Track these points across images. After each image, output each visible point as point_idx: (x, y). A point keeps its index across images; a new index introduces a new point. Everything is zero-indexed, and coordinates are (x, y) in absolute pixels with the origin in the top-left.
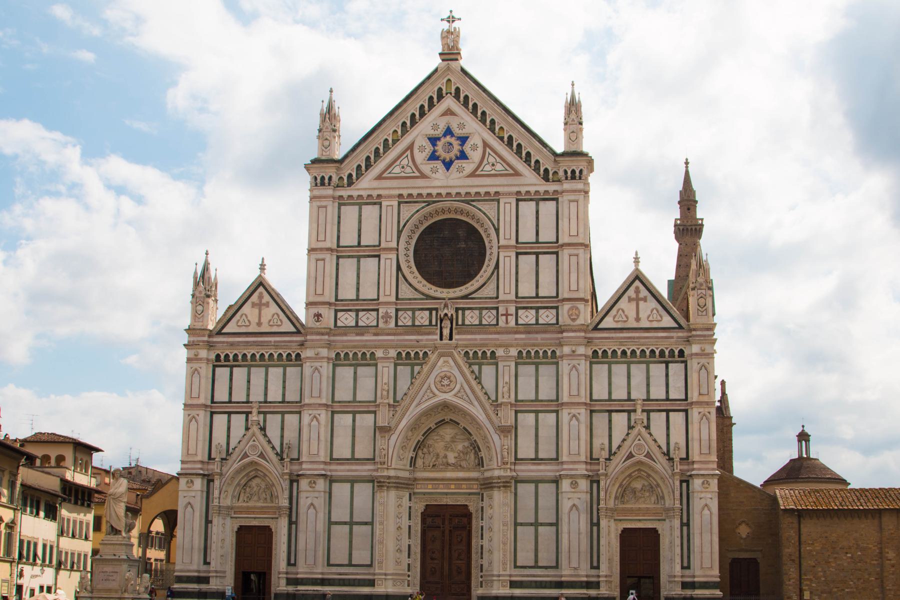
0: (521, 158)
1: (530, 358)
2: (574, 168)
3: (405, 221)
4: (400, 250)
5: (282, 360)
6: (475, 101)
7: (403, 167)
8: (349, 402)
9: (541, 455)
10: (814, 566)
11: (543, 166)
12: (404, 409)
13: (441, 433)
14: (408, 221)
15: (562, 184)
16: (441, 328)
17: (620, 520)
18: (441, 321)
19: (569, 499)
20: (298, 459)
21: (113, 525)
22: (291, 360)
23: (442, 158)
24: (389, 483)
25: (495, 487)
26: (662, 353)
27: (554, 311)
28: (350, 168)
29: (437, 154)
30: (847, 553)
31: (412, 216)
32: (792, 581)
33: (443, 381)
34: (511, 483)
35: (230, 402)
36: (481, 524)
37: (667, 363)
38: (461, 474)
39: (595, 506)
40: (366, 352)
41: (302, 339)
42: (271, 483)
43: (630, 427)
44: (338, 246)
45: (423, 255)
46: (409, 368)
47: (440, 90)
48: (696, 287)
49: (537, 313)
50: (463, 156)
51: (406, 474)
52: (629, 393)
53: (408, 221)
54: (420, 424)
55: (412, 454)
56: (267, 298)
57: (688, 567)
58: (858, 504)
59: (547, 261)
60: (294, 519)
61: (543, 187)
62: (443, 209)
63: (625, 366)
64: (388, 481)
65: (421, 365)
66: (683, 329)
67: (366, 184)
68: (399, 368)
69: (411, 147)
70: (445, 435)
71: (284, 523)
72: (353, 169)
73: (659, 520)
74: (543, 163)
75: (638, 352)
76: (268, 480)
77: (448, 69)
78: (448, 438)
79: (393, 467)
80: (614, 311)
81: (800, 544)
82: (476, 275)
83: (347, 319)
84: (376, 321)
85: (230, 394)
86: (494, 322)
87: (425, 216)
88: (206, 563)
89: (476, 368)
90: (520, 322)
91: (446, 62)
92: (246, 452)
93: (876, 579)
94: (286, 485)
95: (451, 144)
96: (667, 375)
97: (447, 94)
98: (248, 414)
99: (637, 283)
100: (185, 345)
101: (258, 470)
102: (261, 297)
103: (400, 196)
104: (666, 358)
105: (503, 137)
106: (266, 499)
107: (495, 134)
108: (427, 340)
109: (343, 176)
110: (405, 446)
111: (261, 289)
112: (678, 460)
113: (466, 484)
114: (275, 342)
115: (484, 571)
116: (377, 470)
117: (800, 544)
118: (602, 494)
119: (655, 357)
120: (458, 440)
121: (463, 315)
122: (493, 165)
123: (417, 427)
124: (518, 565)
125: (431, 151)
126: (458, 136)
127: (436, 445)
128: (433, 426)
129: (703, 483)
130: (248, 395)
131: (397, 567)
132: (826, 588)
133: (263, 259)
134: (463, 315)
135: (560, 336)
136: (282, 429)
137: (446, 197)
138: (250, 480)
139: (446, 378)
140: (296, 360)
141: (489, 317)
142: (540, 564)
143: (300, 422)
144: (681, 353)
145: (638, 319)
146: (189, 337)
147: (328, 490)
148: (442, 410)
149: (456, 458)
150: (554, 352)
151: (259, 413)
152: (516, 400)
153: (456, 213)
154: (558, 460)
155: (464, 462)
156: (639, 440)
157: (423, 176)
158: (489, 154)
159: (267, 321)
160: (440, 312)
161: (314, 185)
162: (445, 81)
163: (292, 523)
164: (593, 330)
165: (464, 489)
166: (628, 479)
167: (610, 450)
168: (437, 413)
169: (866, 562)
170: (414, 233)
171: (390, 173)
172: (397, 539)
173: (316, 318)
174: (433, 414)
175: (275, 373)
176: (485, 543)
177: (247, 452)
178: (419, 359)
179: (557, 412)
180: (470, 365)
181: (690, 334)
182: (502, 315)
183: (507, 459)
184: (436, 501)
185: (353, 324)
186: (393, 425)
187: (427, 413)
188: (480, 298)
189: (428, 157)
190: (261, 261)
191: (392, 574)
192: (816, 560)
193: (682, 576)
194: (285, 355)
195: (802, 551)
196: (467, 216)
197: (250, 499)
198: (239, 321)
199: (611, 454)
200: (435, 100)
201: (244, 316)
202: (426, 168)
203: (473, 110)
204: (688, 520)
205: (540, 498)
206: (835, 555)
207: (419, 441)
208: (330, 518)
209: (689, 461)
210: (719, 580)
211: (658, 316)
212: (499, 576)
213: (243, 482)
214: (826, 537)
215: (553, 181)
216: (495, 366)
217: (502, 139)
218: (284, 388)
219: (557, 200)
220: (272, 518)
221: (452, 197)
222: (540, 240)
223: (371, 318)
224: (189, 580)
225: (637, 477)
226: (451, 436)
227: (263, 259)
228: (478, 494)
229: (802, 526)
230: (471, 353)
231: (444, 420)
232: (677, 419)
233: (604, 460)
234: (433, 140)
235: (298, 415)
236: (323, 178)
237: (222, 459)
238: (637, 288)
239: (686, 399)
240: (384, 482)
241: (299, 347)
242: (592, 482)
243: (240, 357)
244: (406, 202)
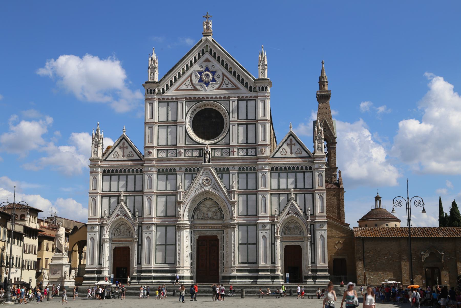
0: (240, 81)
1: (244, 171)
2: (263, 86)
3: (188, 109)
4: (186, 123)
5: (134, 172)
6: (219, 55)
7: (187, 85)
8: (164, 191)
9: (249, 214)
10: (370, 262)
11: (249, 85)
12: (189, 193)
13: (205, 204)
14: (189, 110)
15: (258, 93)
16: (205, 158)
17: (284, 242)
18: (205, 154)
20: (142, 216)
21: (58, 249)
22: (138, 172)
23: (204, 81)
26: (302, 168)
27: (254, 150)
28: (163, 86)
29: (202, 79)
30: (385, 257)
31: (191, 107)
33: (206, 181)
35: (110, 191)
36: (223, 244)
37: (304, 172)
38: (214, 222)
39: (273, 236)
40: (172, 168)
41: (143, 163)
42: (129, 227)
43: (288, 201)
44: (158, 121)
46: (191, 175)
47: (203, 50)
48: (317, 139)
49: (247, 150)
50: (214, 80)
52: (287, 186)
53: (189, 110)
55: (192, 213)
56: (126, 144)
57: (314, 263)
58: (390, 235)
59: (251, 127)
60: (140, 243)
61: (249, 94)
63: (286, 174)
64: (182, 226)
65: (196, 174)
66: (311, 157)
67: (171, 93)
68: (186, 175)
69: (191, 76)
70: (207, 205)
71: (136, 245)
72: (165, 86)
73: (301, 242)
74: (249, 84)
75: (291, 168)
76: (128, 226)
77: (207, 40)
78: (208, 206)
79: (184, 219)
80: (281, 150)
81: (364, 252)
82: (220, 133)
83: (163, 155)
84: (176, 154)
85: (110, 188)
86: (228, 155)
87: (197, 107)
88: (100, 264)
89: (220, 175)
90: (240, 154)
91: (205, 37)
92: (118, 214)
93: (398, 268)
94: (136, 228)
95: (208, 76)
96: (304, 178)
97: (206, 52)
98: (119, 197)
99: (291, 137)
100: (89, 166)
101: (123, 222)
102: (124, 144)
103: (186, 98)
104: (304, 170)
105: (232, 72)
106: (127, 235)
107: (228, 70)
108: (199, 163)
109: (160, 89)
111: (124, 140)
112: (309, 215)
113: (217, 226)
114: (130, 164)
115: (225, 265)
116: (177, 221)
117: (364, 252)
118: (276, 230)
119: (299, 170)
120: (213, 207)
121: (214, 152)
122: (227, 84)
123: (195, 201)
125: (199, 78)
126: (212, 71)
128: (201, 200)
129: (320, 226)
130: (118, 188)
134: (214, 152)
135: (257, 161)
136: (134, 203)
137: (206, 99)
138: (120, 226)
139: (207, 180)
140: (140, 172)
141: (226, 152)
142: (249, 262)
143: (142, 200)
144: (310, 168)
145: (291, 153)
146: (91, 162)
150: (254, 168)
153: (211, 106)
154: (257, 215)
155: (215, 216)
156: (292, 206)
157: (196, 89)
158: (225, 79)
159: (127, 155)
160: (204, 151)
161: (147, 93)
162: (205, 45)
163: (140, 245)
164: (271, 158)
165: (216, 229)
166: (287, 223)
167: (279, 211)
170: (192, 115)
171: (181, 88)
172: (186, 251)
173: (149, 153)
174: (202, 196)
175: (131, 178)
176: (225, 252)
177: (118, 214)
178: (195, 171)
179: (256, 194)
180: (218, 174)
181: (314, 160)
182: (232, 152)
184: (203, 234)
185: (165, 156)
187: (199, 195)
188: (222, 144)
189: (198, 81)
193: (312, 267)
194: (135, 170)
195: (364, 255)
196: (216, 107)
197: (120, 235)
198: (114, 155)
199: (280, 212)
200: (201, 54)
201: (116, 152)
202: (198, 87)
203: (218, 59)
204: (314, 241)
205: (249, 232)
206: (380, 258)
207: (195, 208)
208: (156, 243)
209: (314, 216)
210: (328, 268)
211: (300, 152)
212: (231, 267)
213: (116, 227)
214: (375, 249)
215: (254, 92)
216: (229, 174)
217: (231, 72)
218: (135, 185)
219: (255, 100)
220: (130, 243)
221: (209, 99)
222: (248, 118)
223: (174, 153)
224: (93, 272)
225: (292, 223)
226: (210, 205)
228: (222, 231)
229: (364, 244)
230: (218, 169)
231: (206, 198)
232: (309, 197)
233: (277, 215)
234: (200, 73)
235: (141, 197)
236: (151, 90)
237: (107, 217)
238: (291, 139)
239: (313, 188)
240: (180, 226)
241: (141, 166)
242: (271, 225)
243: (115, 171)
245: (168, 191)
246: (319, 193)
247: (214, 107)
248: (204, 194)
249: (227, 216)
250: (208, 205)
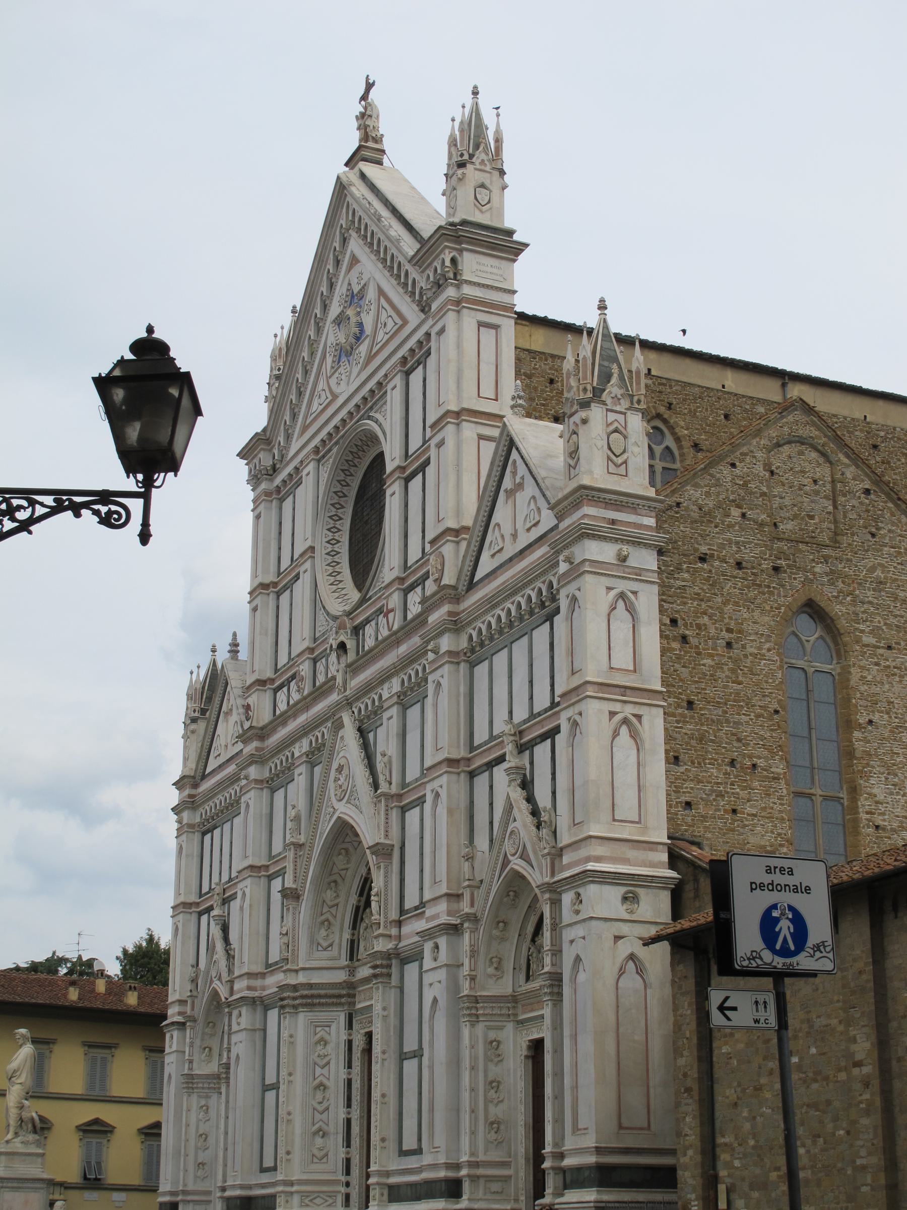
24: (295, 998)
32: (690, 1152)
34: (389, 966)
51: (340, 976)
79: (301, 965)
87: (343, 470)
110: (327, 920)
124: (405, 1148)
131: (314, 1167)
132: (758, 1171)
133: (235, 635)
147: (258, 1026)
151: (224, 903)
152: (404, 785)
169: (826, 1078)
188: (376, 593)
190: (231, 638)
191: (300, 1182)
192: (739, 1085)
227: (235, 635)
244: (324, 456)
246: (568, 716)
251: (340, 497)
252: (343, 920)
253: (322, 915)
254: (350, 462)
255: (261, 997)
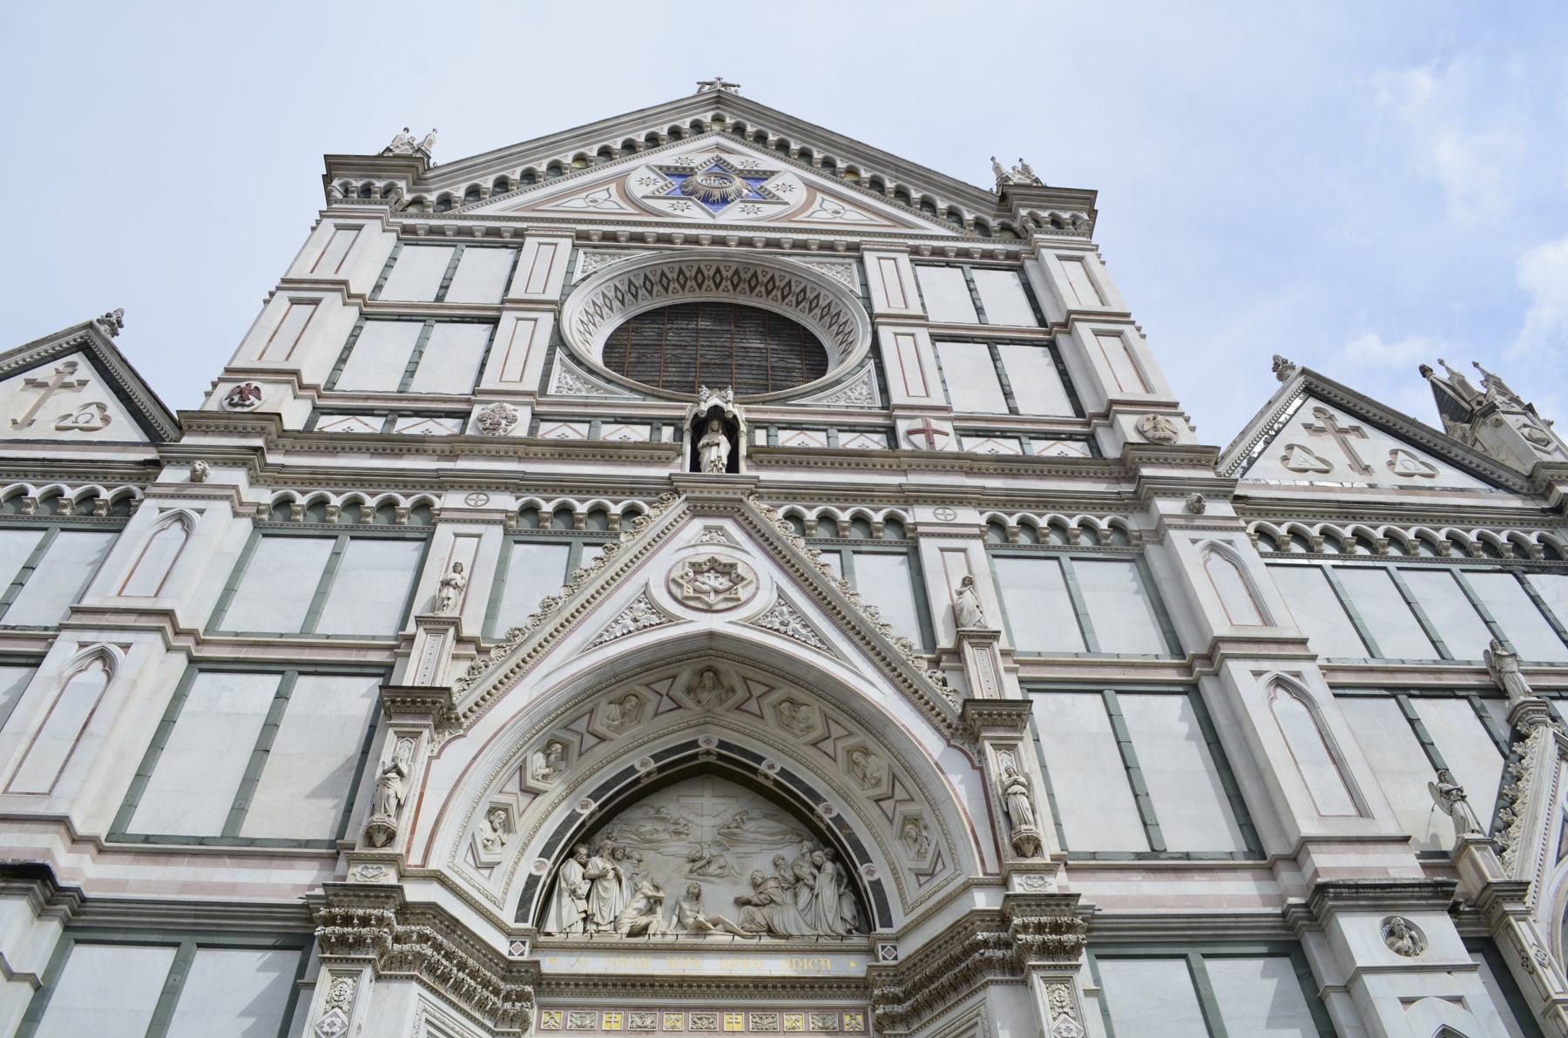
14: (595, 272)
19: (1407, 1001)
23: (702, 193)
25: (989, 964)
45: (635, 355)
54: (591, 740)
55: (532, 864)
62: (699, 271)
70: (690, 817)
87: (646, 277)
127: (649, 856)
128: (643, 764)
148: (689, 690)
149: (741, 903)
153: (735, 287)
158: (823, 200)
168: (666, 704)
174: (654, 698)
183: (1033, 827)
186: (463, 702)
226: (719, 821)
231: (694, 744)
245: (319, 636)
247: (759, 295)
248: (678, 692)
249: (932, 875)
250: (698, 820)
251: (616, 297)
252: (536, 829)
253: (501, 792)
254: (664, 279)
255: (84, 900)
